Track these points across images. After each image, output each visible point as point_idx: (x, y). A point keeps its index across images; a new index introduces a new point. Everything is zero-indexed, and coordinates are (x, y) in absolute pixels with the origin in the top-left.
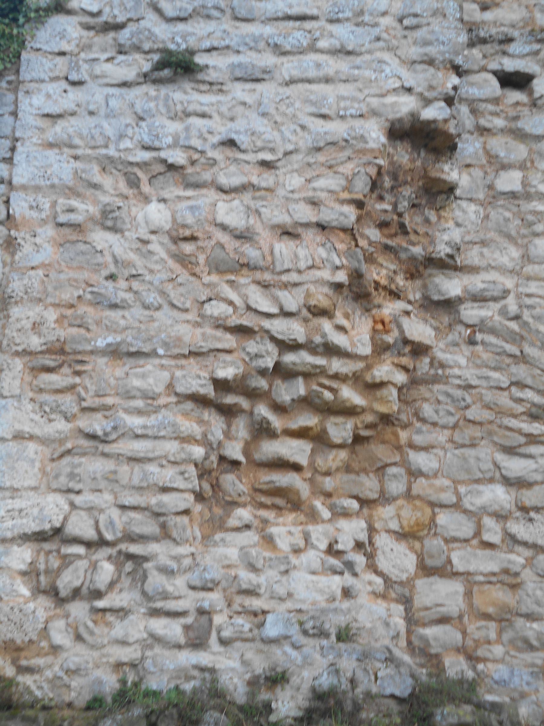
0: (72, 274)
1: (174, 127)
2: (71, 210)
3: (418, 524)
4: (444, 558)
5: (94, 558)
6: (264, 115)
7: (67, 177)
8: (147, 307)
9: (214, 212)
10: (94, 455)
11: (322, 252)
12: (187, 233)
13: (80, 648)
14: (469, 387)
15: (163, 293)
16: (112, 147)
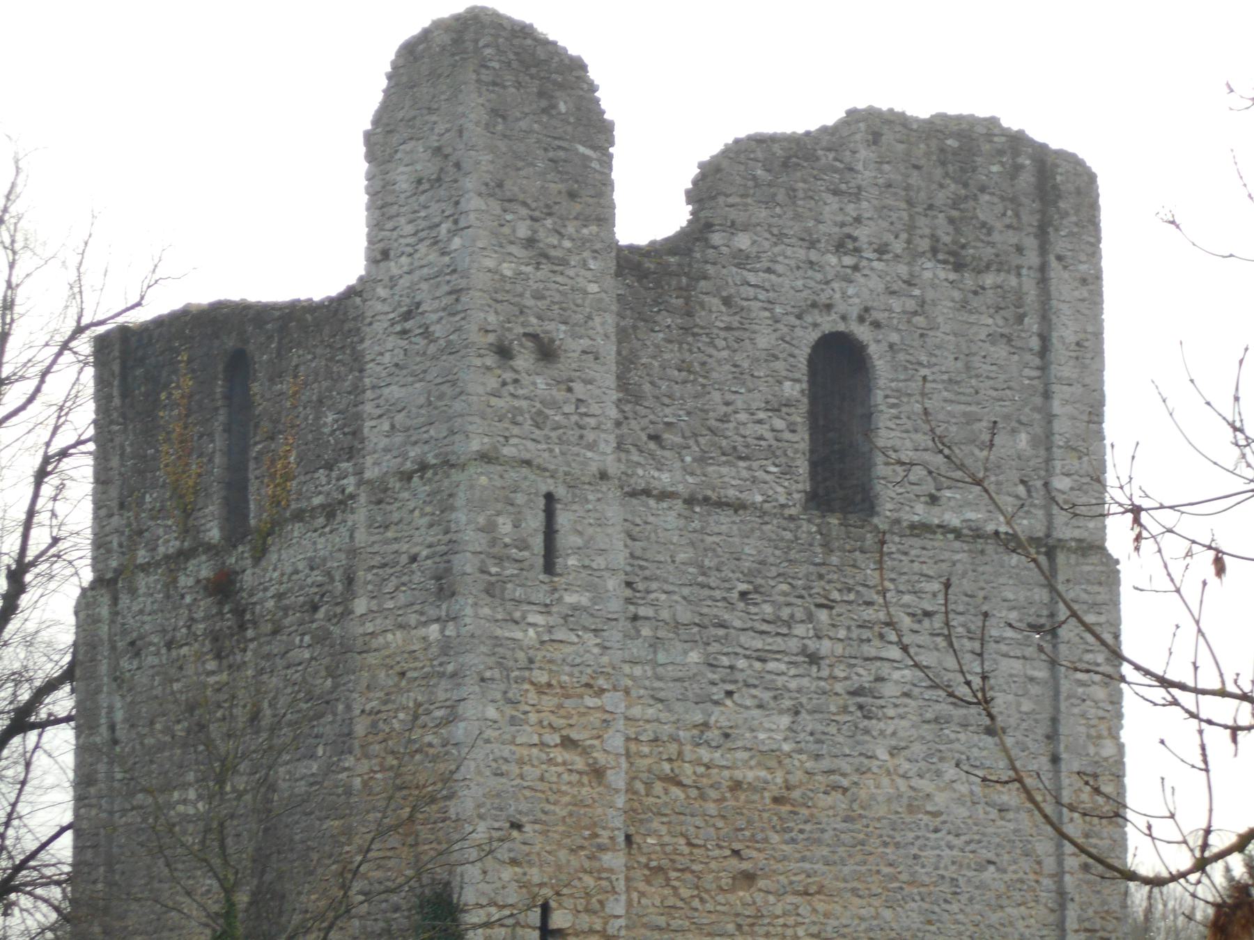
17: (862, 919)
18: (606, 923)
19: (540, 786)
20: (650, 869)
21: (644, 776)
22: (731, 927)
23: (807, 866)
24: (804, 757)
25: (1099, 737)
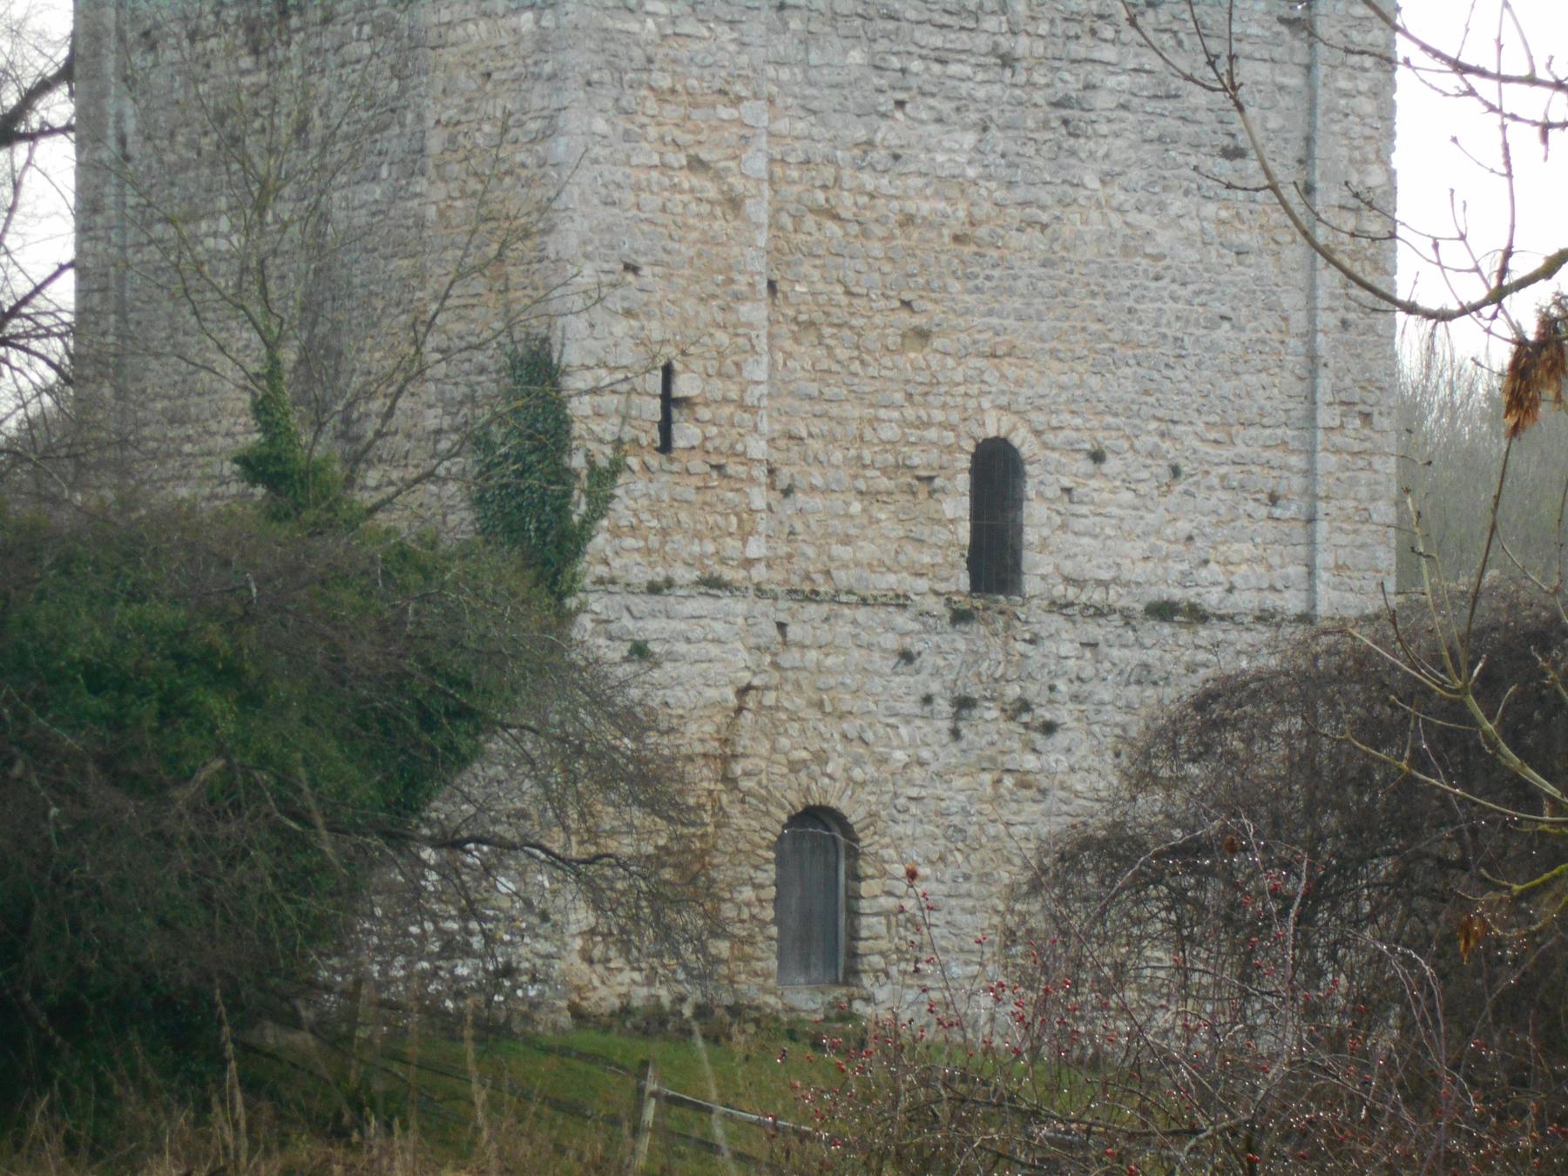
14: (740, 830)
17: (1062, 388)
18: (743, 391)
19: (661, 218)
20: (798, 323)
21: (792, 208)
22: (899, 397)
23: (995, 321)
24: (993, 185)
25: (1365, 161)
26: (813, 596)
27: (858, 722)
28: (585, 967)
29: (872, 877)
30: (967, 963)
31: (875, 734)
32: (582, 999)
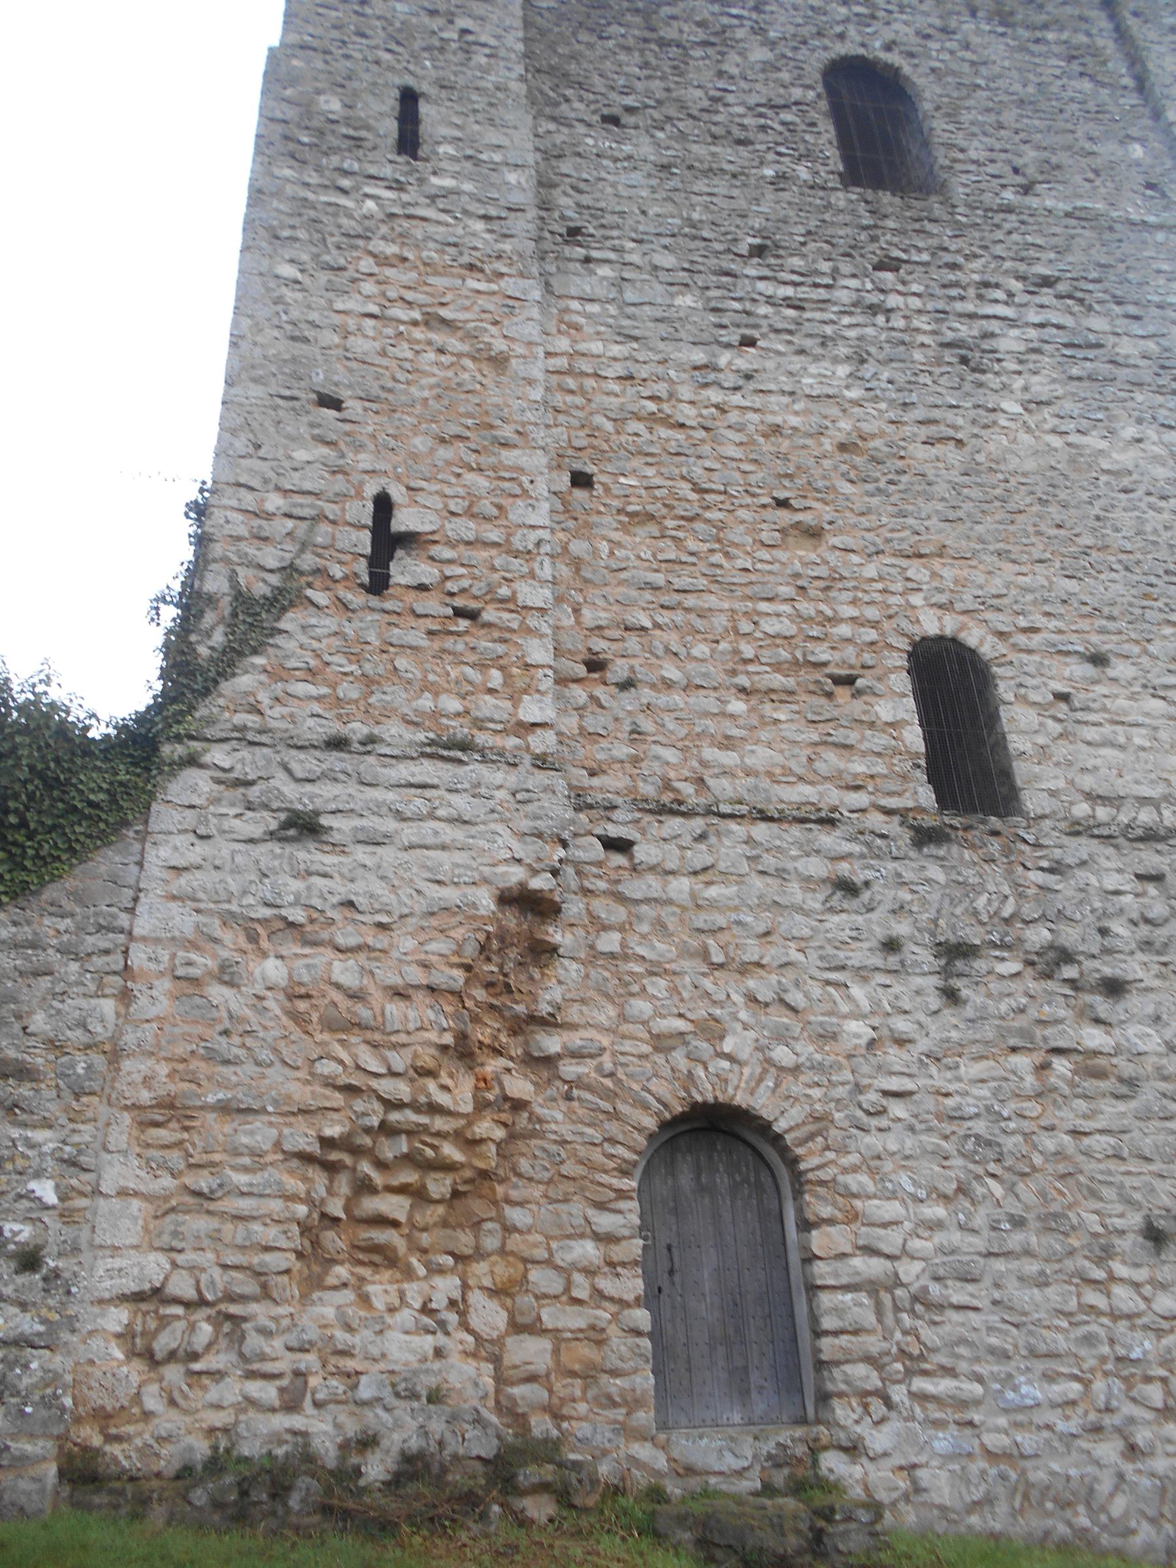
0: (187, 1028)
1: (296, 885)
2: (189, 964)
3: (510, 1281)
4: (534, 1314)
5: (192, 1318)
6: (382, 878)
7: (189, 931)
8: (258, 1064)
9: (330, 971)
10: (198, 1212)
11: (431, 1014)
12: (303, 991)
13: (173, 1414)
14: (564, 1142)
15: (275, 1050)
16: (235, 902)
17: (1026, 590)
19: (379, 360)
20: (628, 514)
22: (786, 590)
23: (910, 521)
24: (883, 406)
26: (675, 809)
27: (774, 978)
28: (134, 1371)
29: (831, 1222)
30: (1050, 1377)
31: (807, 995)
32: (110, 1439)
